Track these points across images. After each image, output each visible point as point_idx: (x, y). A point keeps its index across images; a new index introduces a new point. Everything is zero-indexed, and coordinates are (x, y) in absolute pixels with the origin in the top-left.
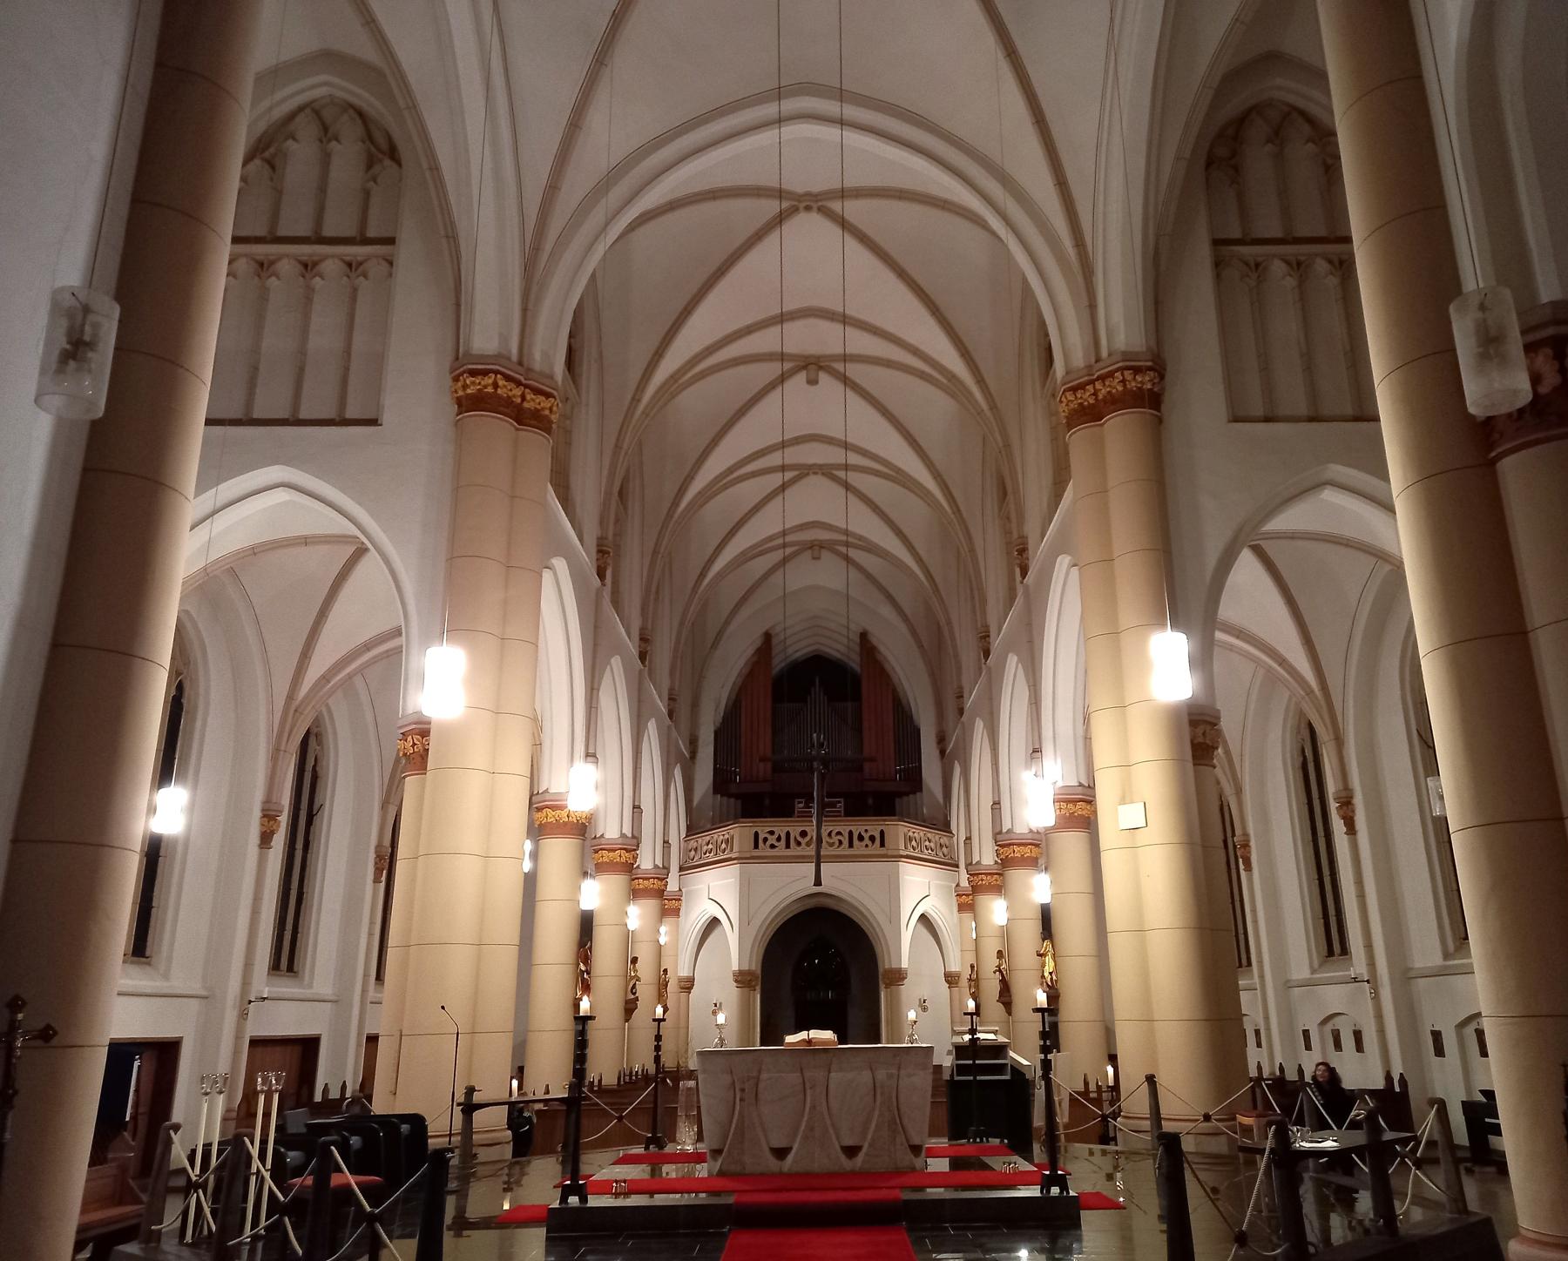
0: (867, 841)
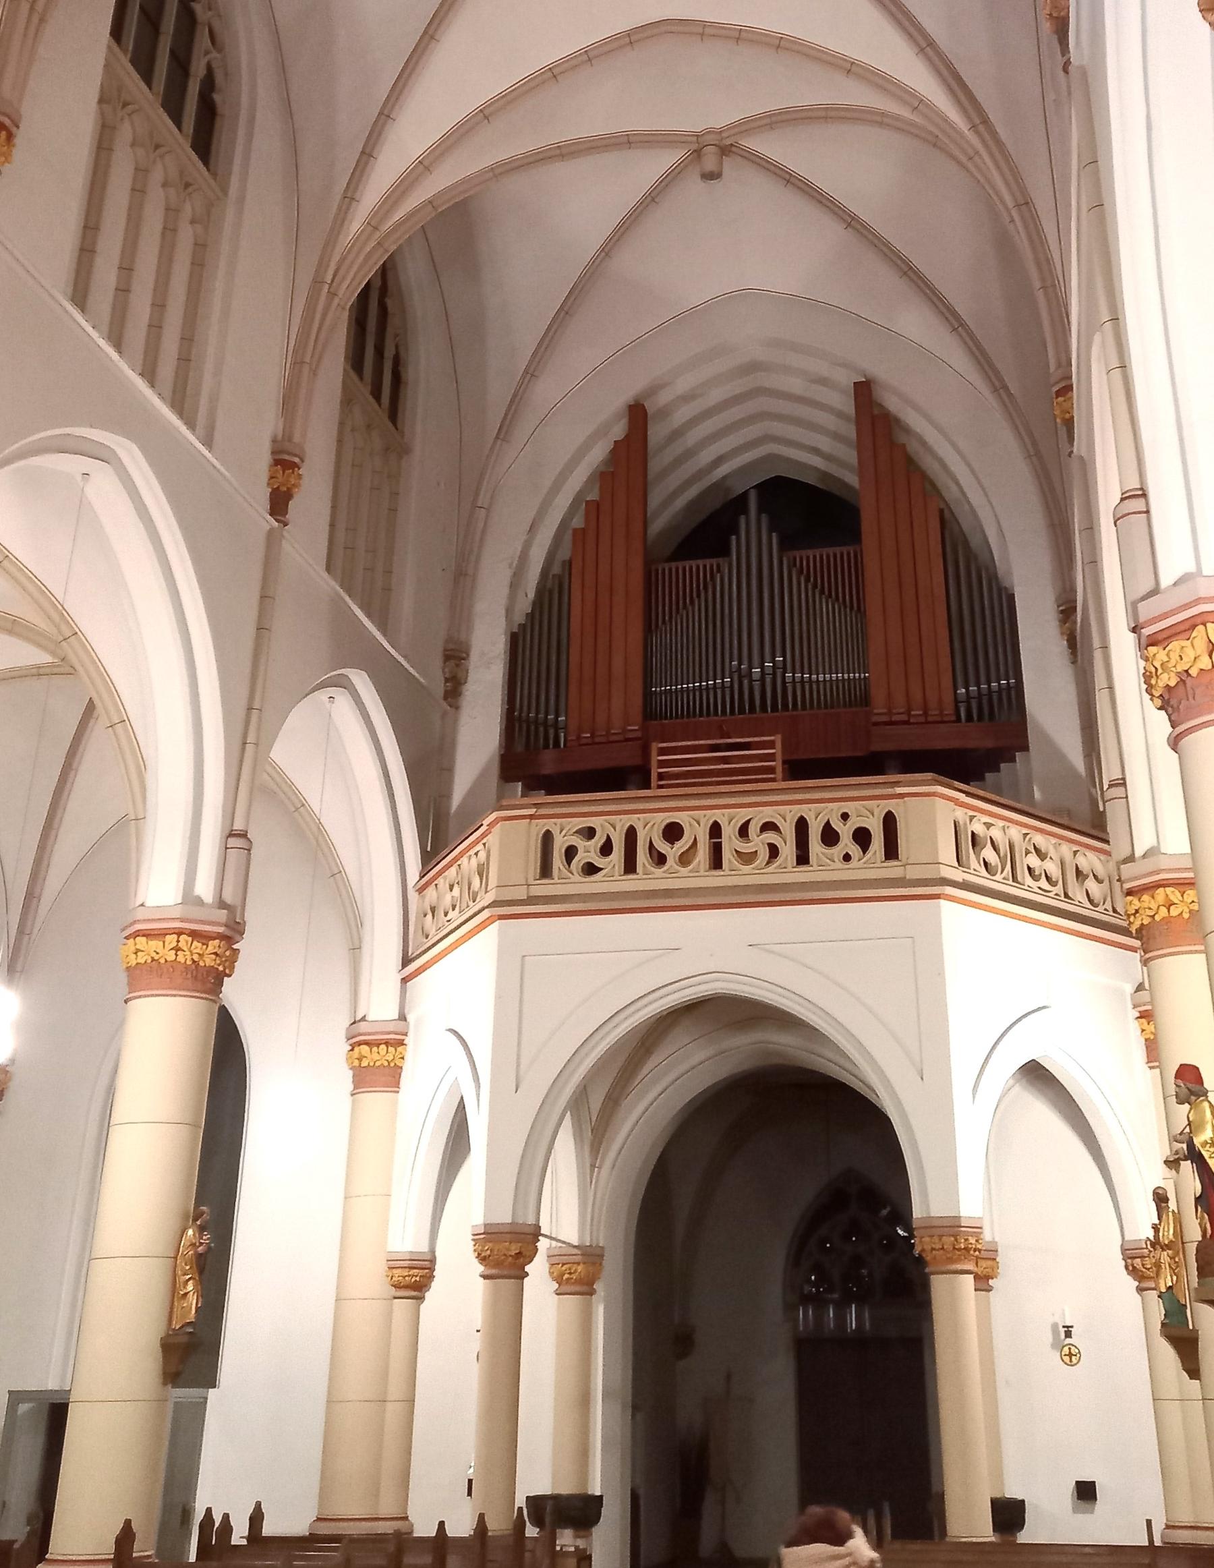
0: (847, 843)
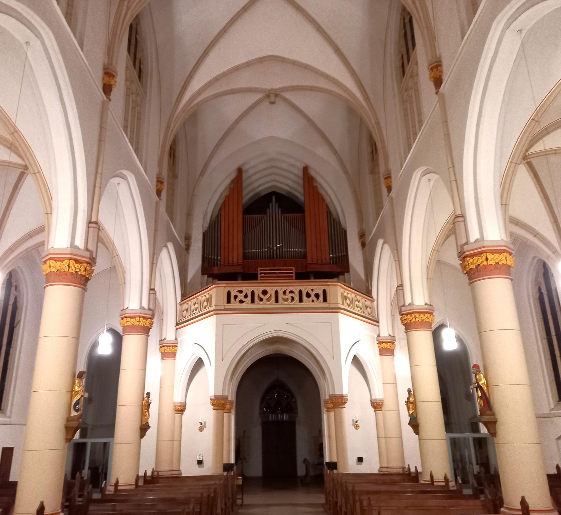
0: (313, 297)
